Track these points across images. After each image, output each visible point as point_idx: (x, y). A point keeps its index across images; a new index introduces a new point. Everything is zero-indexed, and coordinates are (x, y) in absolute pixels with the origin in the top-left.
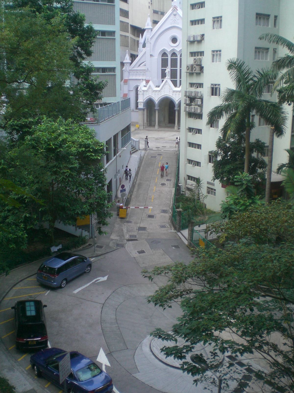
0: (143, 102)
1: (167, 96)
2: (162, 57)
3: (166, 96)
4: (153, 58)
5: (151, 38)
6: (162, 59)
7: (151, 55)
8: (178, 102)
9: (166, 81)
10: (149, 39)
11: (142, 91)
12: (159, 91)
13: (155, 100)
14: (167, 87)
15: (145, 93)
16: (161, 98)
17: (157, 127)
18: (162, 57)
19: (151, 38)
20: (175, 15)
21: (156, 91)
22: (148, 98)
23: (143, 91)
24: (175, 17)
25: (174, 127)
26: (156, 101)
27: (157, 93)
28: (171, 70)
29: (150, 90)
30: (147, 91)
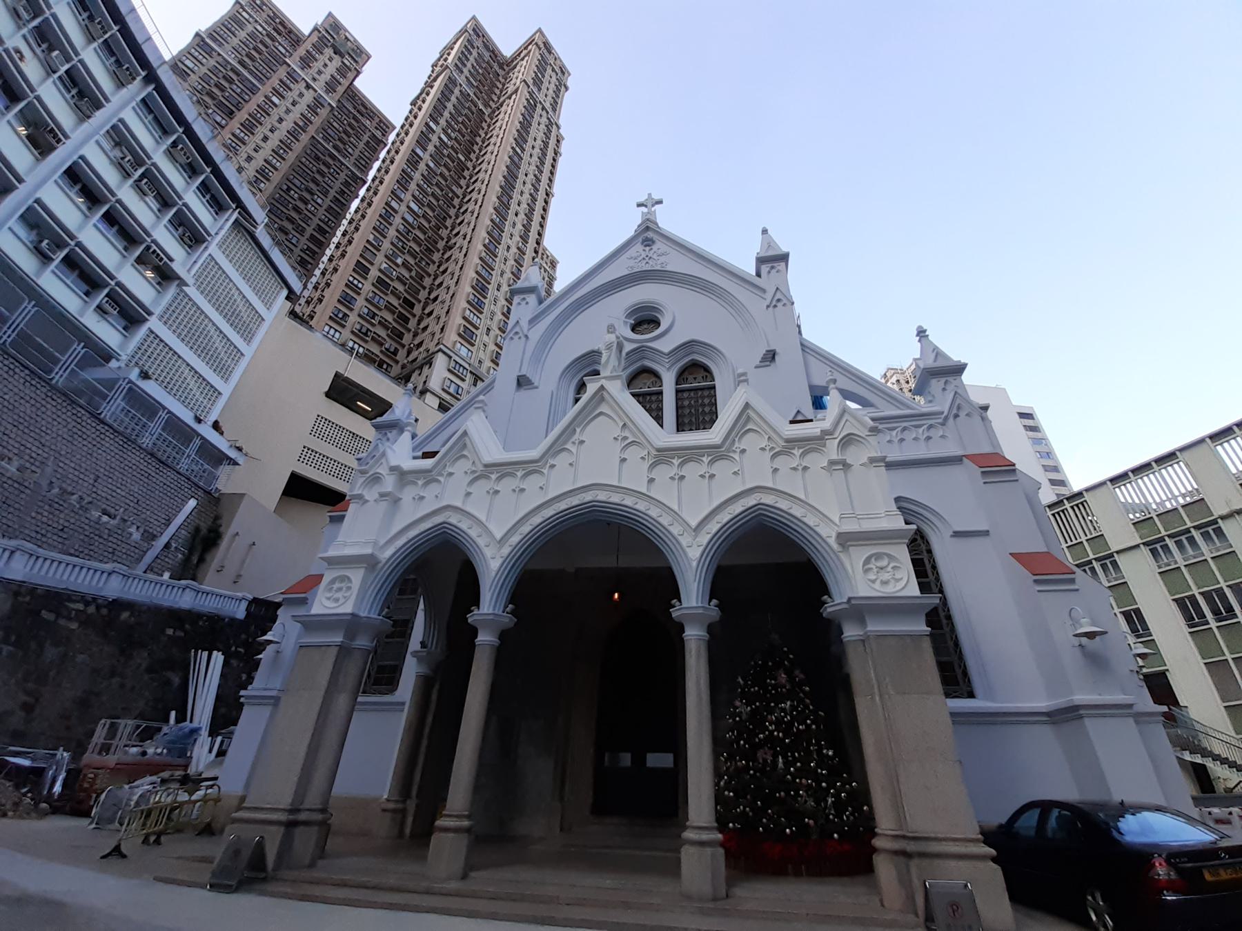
1: (602, 496)
3: (588, 497)
4: (524, 393)
5: (533, 321)
7: (522, 382)
8: (704, 539)
10: (524, 324)
12: (531, 468)
16: (537, 520)
19: (533, 321)
20: (648, 243)
24: (648, 248)
26: (488, 552)
27: (507, 485)
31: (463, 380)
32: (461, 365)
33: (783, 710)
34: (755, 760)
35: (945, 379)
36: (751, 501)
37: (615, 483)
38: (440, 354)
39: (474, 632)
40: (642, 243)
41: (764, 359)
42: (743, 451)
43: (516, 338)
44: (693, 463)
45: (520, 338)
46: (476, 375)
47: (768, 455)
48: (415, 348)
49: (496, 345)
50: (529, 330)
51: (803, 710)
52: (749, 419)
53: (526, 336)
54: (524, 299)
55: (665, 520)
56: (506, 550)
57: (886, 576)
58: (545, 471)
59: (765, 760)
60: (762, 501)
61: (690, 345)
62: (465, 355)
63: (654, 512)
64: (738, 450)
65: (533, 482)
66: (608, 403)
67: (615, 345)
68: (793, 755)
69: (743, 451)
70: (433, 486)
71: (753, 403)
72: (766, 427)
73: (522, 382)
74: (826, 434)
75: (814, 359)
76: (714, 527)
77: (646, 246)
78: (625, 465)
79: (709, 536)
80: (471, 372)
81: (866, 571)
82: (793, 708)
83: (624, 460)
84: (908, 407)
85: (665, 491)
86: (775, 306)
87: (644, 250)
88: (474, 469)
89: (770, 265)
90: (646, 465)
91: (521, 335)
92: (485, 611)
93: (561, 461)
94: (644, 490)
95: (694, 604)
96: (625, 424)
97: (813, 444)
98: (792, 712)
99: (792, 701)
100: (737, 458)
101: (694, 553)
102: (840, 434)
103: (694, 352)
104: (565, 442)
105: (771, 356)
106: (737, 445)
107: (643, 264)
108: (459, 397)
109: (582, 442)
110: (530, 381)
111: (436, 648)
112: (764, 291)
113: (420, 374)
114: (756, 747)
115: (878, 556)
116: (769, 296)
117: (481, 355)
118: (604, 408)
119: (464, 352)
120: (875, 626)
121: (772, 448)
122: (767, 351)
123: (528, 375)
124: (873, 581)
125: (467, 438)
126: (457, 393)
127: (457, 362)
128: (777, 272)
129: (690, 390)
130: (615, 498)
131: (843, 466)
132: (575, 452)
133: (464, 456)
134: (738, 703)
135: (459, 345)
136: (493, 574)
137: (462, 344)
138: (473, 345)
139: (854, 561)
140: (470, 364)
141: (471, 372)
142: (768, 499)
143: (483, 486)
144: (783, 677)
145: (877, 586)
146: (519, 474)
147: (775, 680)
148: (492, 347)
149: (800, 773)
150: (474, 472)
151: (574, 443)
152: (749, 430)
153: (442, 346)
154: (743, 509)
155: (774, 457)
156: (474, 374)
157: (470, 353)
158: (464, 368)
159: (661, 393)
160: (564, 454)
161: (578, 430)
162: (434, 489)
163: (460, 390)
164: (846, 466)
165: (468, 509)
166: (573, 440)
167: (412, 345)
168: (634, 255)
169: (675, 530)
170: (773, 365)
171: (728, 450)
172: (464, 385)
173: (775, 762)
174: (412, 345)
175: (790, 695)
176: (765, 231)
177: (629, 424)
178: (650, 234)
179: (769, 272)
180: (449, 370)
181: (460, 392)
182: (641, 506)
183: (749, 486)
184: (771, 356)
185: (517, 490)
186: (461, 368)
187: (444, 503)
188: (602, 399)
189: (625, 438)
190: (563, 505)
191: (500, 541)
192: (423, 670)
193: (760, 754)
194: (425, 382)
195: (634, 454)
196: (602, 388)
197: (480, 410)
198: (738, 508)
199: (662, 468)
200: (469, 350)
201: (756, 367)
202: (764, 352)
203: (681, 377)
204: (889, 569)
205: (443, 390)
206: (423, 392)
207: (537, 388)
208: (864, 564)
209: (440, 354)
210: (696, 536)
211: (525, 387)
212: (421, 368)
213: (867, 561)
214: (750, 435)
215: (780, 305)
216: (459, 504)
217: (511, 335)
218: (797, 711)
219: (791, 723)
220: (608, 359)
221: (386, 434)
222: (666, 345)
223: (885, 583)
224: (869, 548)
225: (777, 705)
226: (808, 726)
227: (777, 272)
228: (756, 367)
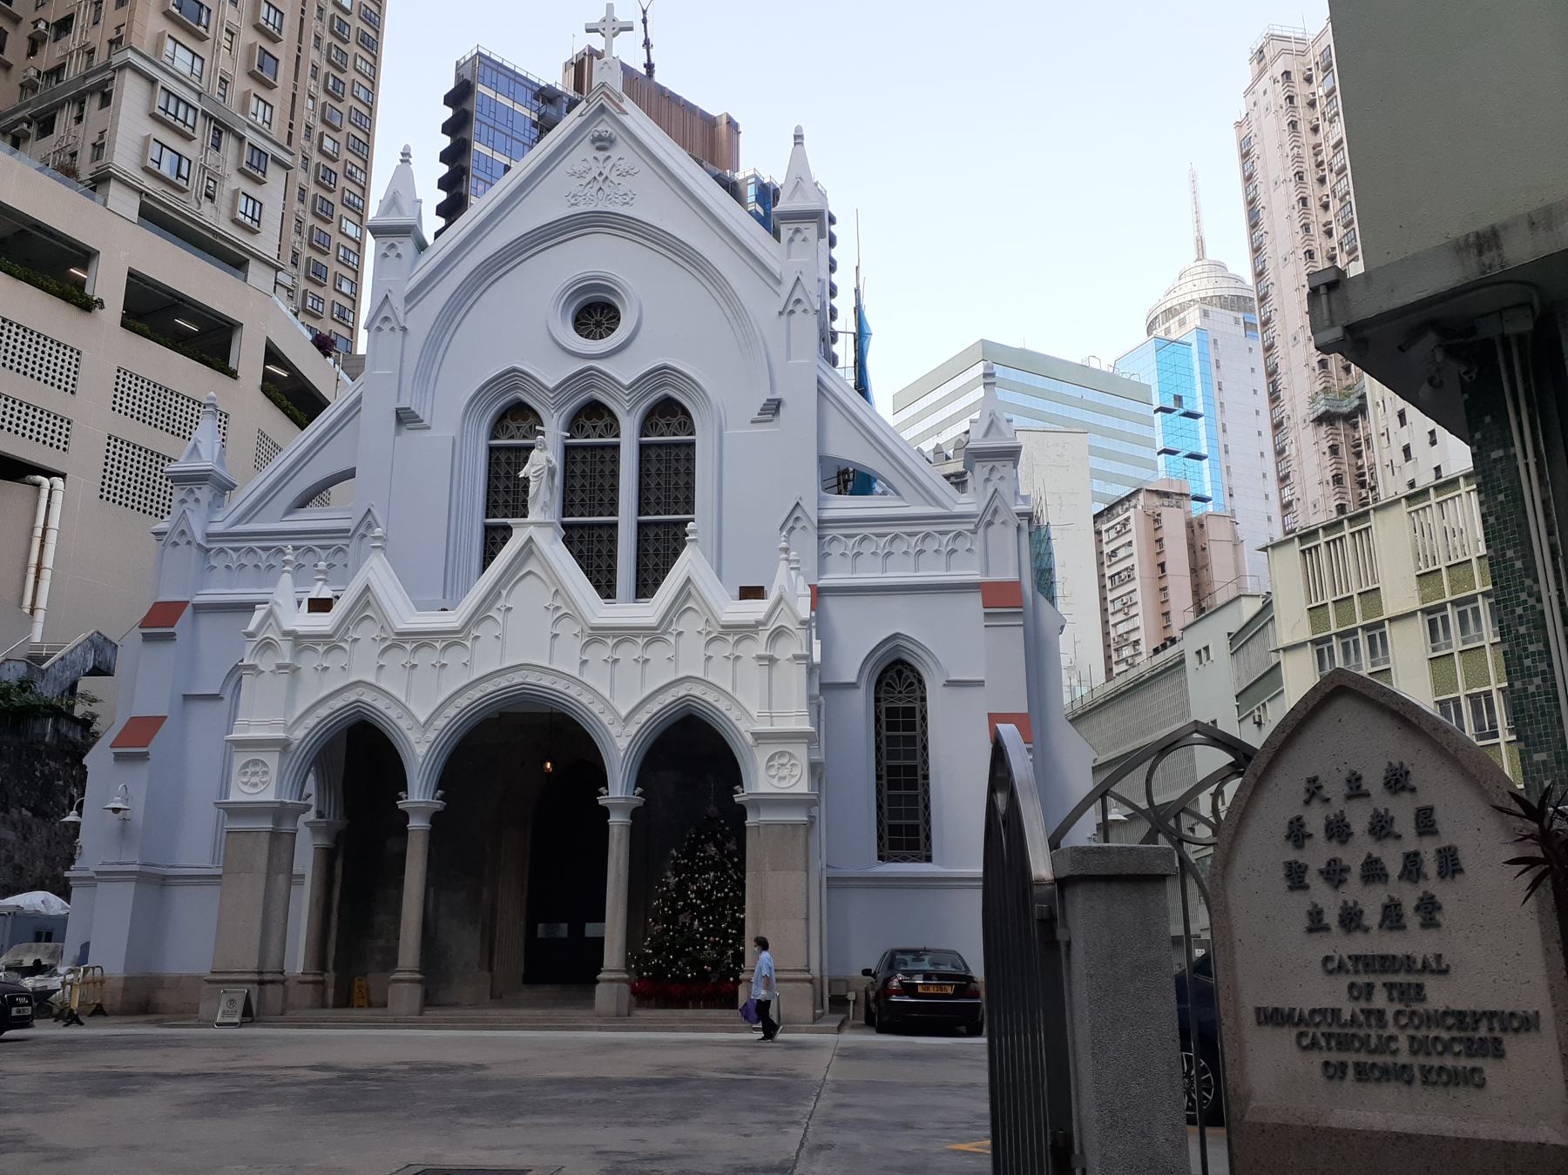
0: (283, 746)
1: (532, 678)
2: (493, 436)
3: (517, 678)
4: (410, 436)
5: (412, 297)
6: (492, 450)
7: (405, 418)
8: (633, 729)
9: (529, 548)
10: (397, 301)
11: (286, 647)
12: (452, 639)
13: (403, 724)
14: (528, 598)
15: (308, 662)
17: (404, 994)
18: (493, 435)
20: (603, 143)
21: (423, 639)
22: (338, 703)
23: (296, 638)
24: (601, 155)
25: (587, 999)
26: (413, 736)
27: (425, 658)
28: (568, 450)
29: (367, 632)
30: (329, 642)
31: (188, 138)
32: (179, 100)
33: (707, 880)
34: (675, 924)
35: (991, 464)
36: (681, 691)
37: (546, 664)
38: (128, 74)
39: (405, 816)
40: (594, 141)
41: (764, 411)
42: (680, 633)
43: (386, 327)
44: (628, 644)
45: (392, 329)
46: (217, 121)
47: (703, 640)
48: (51, 34)
49: (259, 28)
50: (406, 313)
51: (725, 880)
52: (689, 594)
53: (404, 329)
54: (392, 246)
55: (596, 708)
56: (432, 735)
57: (784, 772)
58: (468, 644)
59: (684, 924)
60: (692, 692)
61: (662, 373)
62: (186, 70)
63: (585, 699)
64: (675, 633)
65: (454, 657)
66: (537, 558)
67: (546, 469)
68: (708, 919)
69: (680, 633)
70: (336, 654)
71: (696, 578)
72: (706, 610)
73: (405, 418)
74: (758, 623)
75: (835, 411)
76: (643, 717)
77: (599, 149)
78: (557, 641)
79: (638, 726)
80: (205, 114)
81: (769, 767)
82: (716, 878)
83: (556, 636)
84: (939, 503)
85: (597, 679)
86: (792, 312)
87: (595, 158)
88: (384, 635)
89: (796, 226)
90: (579, 644)
91: (394, 324)
92: (416, 799)
93: (483, 631)
94: (575, 673)
95: (619, 796)
96: (557, 591)
97: (744, 631)
98: (714, 882)
99: (716, 872)
100: (673, 641)
101: (622, 743)
102: (771, 626)
103: (666, 384)
104: (489, 608)
105: (773, 408)
106: (674, 626)
107: (594, 193)
108: (182, 183)
109: (509, 609)
110: (418, 417)
111: (335, 818)
112: (779, 282)
113: (79, 119)
114: (677, 912)
115: (782, 754)
116: (785, 290)
117: (225, 63)
118: (531, 566)
119: (182, 61)
120: (767, 816)
121: (709, 633)
122: (768, 400)
123: (413, 409)
124: (773, 777)
125: (369, 594)
126: (179, 175)
127: (169, 93)
128: (803, 240)
129: (659, 445)
130: (546, 681)
131: (770, 661)
132: (501, 622)
133: (367, 617)
134: (669, 874)
135: (169, 44)
136: (420, 760)
137: (177, 42)
138: (201, 38)
139: (762, 755)
140: (200, 94)
141: (205, 114)
142: (697, 691)
143: (397, 659)
144: (712, 850)
145: (775, 782)
146: (439, 645)
147: (704, 852)
148: (248, 37)
149: (708, 932)
150: (384, 639)
151: (499, 609)
152: (689, 608)
153: (130, 55)
154: (673, 699)
155: (709, 643)
156: (212, 118)
157: (197, 63)
158: (188, 105)
159: (616, 447)
160: (488, 623)
161: (504, 593)
162: (335, 661)
163: (185, 164)
164: (772, 660)
165: (382, 685)
166: (498, 605)
167: (42, 26)
168: (579, 167)
169: (605, 719)
170: (775, 418)
171: (665, 632)
172: (189, 151)
173: (692, 924)
174: (42, 26)
175: (714, 867)
176: (798, 138)
177: (561, 590)
178: (604, 127)
179: (791, 240)
180: (154, 116)
181: (184, 173)
182: (573, 691)
183: (682, 674)
184: (773, 408)
185: (438, 665)
186: (182, 107)
187: (353, 679)
188: (531, 552)
189: (558, 608)
190: (489, 687)
191: (425, 724)
192: (322, 841)
193: (681, 918)
194: (98, 148)
195: (567, 629)
196: (530, 539)
197: (378, 550)
198: (667, 698)
199: (595, 647)
200: (194, 54)
201: (752, 422)
202: (764, 401)
203: (648, 424)
204: (788, 766)
205: (146, 170)
206: (100, 181)
207: (429, 428)
208: (769, 761)
209: (128, 74)
210: (624, 727)
211: (409, 426)
212: (80, 100)
213: (772, 758)
214: (690, 613)
215: (799, 309)
216: (371, 679)
217: (377, 323)
218: (720, 881)
219: (710, 892)
220: (538, 490)
221: (191, 491)
222: (625, 371)
223: (782, 778)
224: (774, 746)
225: (700, 876)
226: (726, 894)
227: (803, 240)
228: (752, 422)
